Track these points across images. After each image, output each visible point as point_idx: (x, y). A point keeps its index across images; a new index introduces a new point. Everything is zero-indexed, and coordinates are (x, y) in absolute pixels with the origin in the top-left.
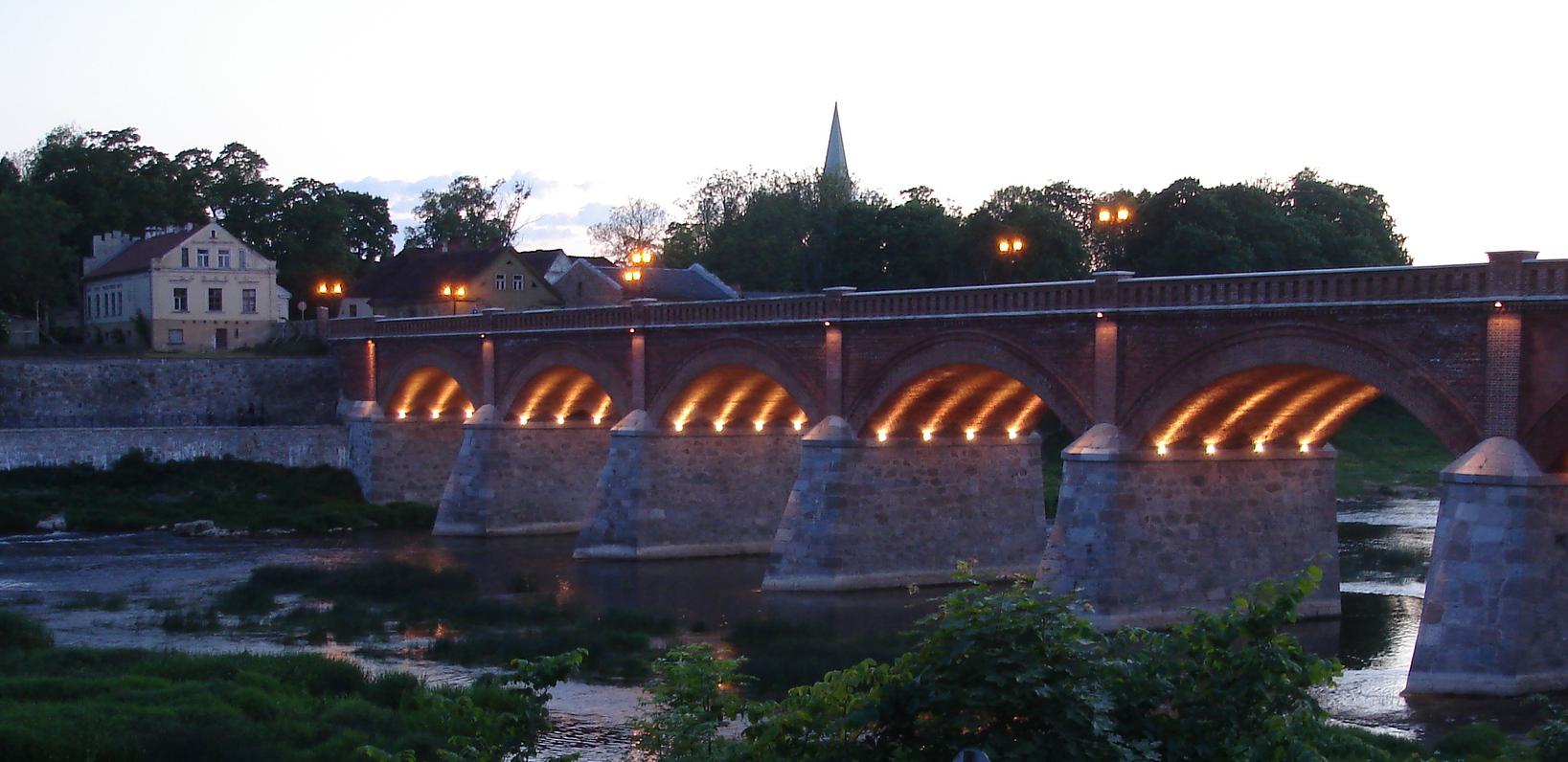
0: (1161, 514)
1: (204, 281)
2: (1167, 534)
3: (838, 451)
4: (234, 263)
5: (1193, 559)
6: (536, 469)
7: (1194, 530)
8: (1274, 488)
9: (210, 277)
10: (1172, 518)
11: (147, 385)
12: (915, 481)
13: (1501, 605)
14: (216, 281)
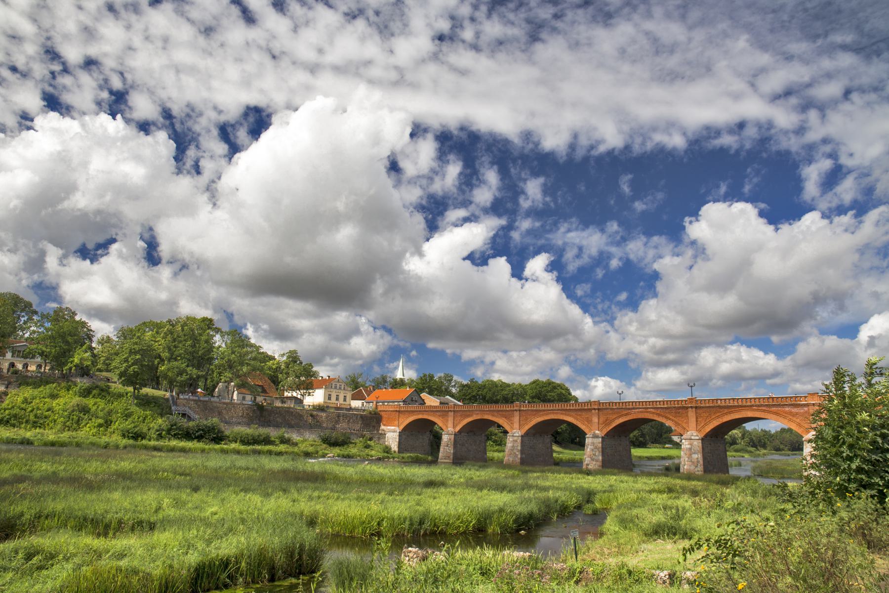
4: (343, 388)
9: (337, 391)
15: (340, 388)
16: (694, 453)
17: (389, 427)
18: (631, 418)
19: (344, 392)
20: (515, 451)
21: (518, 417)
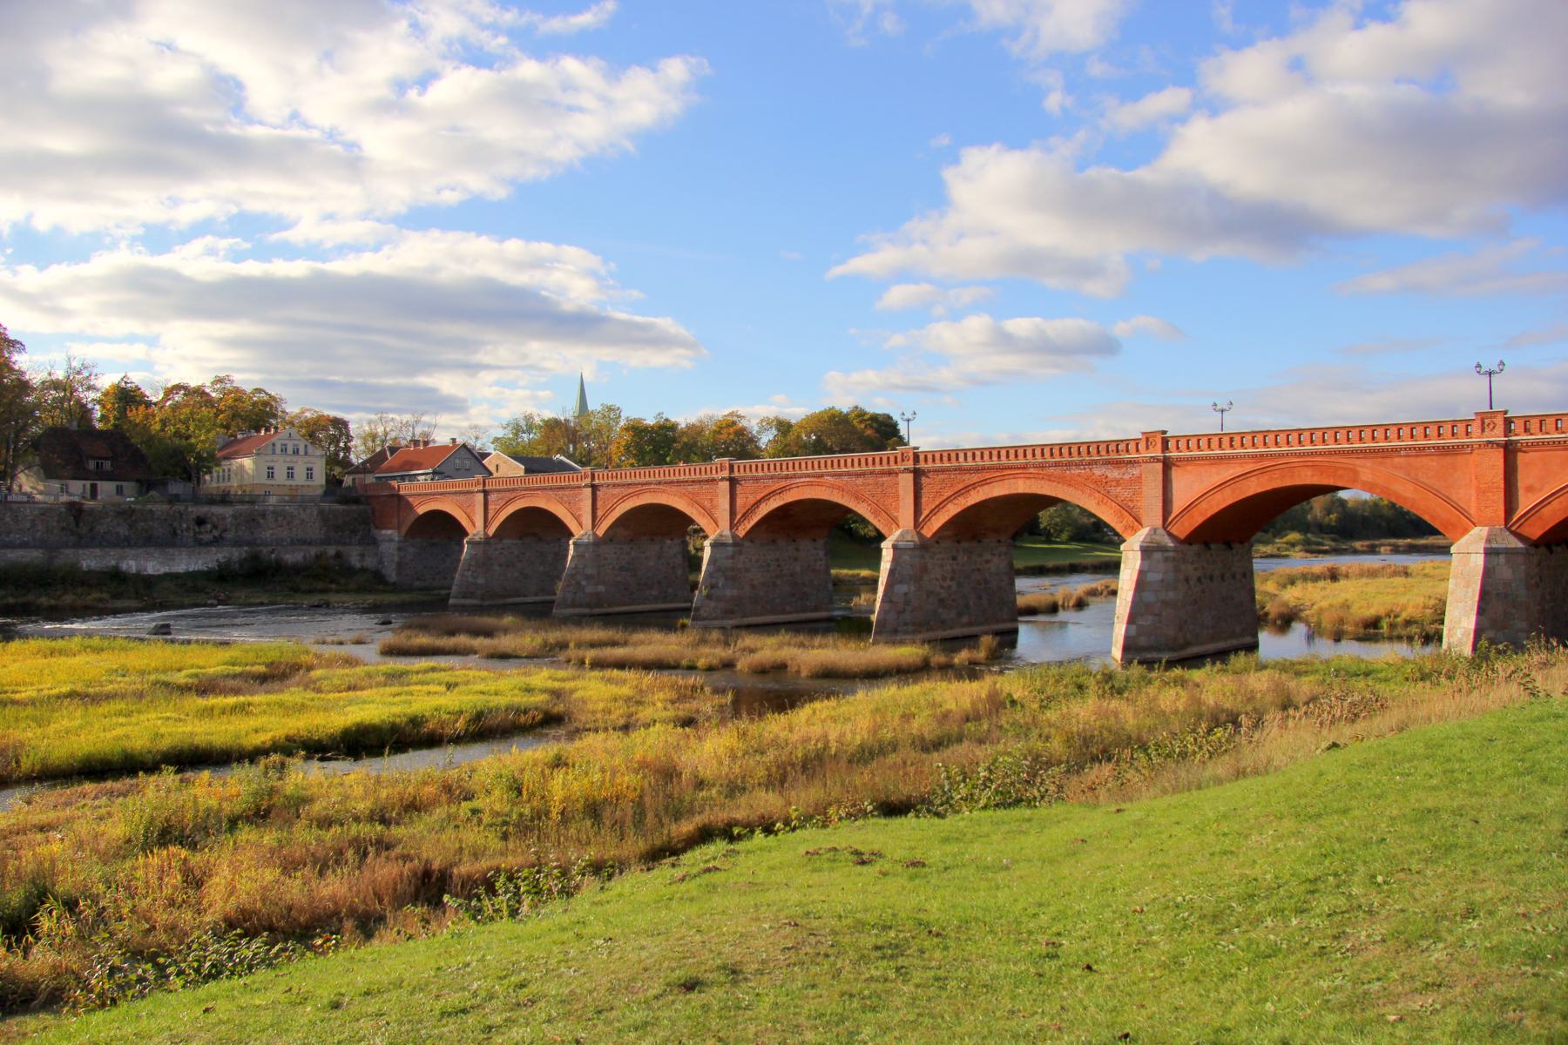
0: (939, 577)
1: (285, 462)
2: (942, 587)
3: (730, 549)
4: (302, 452)
5: (954, 600)
6: (507, 566)
7: (954, 585)
8: (987, 562)
10: (944, 578)
11: (261, 521)
12: (769, 565)
13: (1164, 613)
14: (292, 462)
15: (296, 452)
16: (901, 582)
17: (384, 532)
18: (782, 503)
19: (307, 459)
20: (579, 578)
21: (589, 502)
